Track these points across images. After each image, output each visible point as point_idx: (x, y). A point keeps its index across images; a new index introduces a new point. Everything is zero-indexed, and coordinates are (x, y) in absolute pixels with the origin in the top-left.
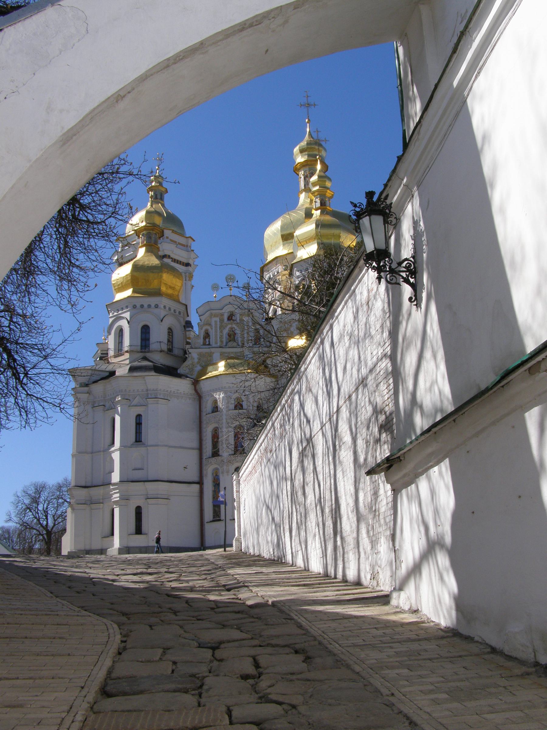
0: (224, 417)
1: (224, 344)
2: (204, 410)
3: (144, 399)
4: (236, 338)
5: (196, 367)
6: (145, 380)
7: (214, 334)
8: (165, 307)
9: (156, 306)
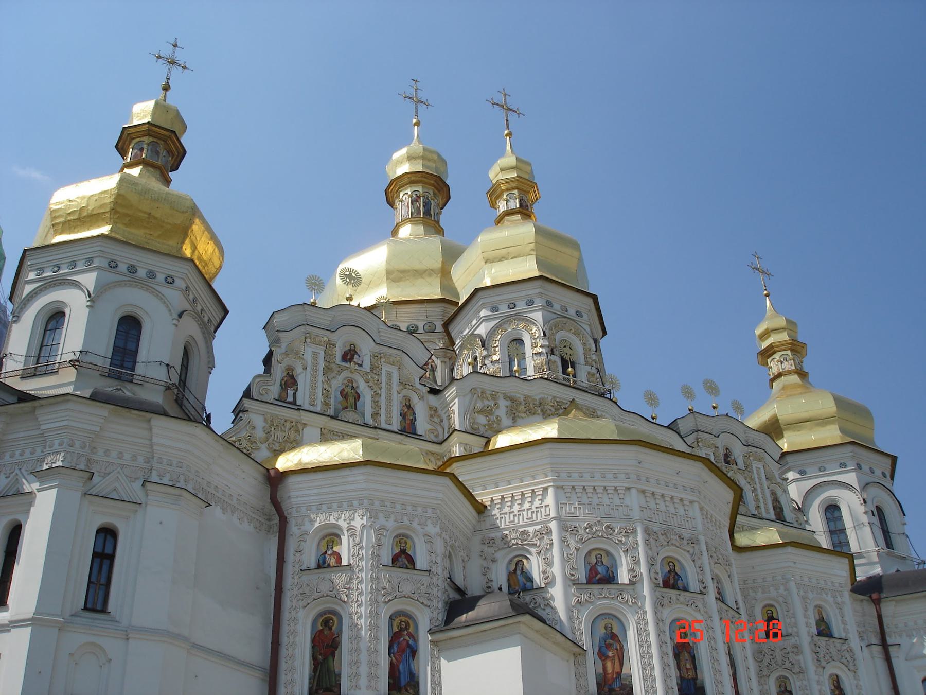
1: (331, 412)
2: (290, 556)
3: (137, 485)
4: (358, 404)
5: (258, 449)
6: (151, 429)
7: (308, 381)
8: (187, 289)
9: (170, 280)
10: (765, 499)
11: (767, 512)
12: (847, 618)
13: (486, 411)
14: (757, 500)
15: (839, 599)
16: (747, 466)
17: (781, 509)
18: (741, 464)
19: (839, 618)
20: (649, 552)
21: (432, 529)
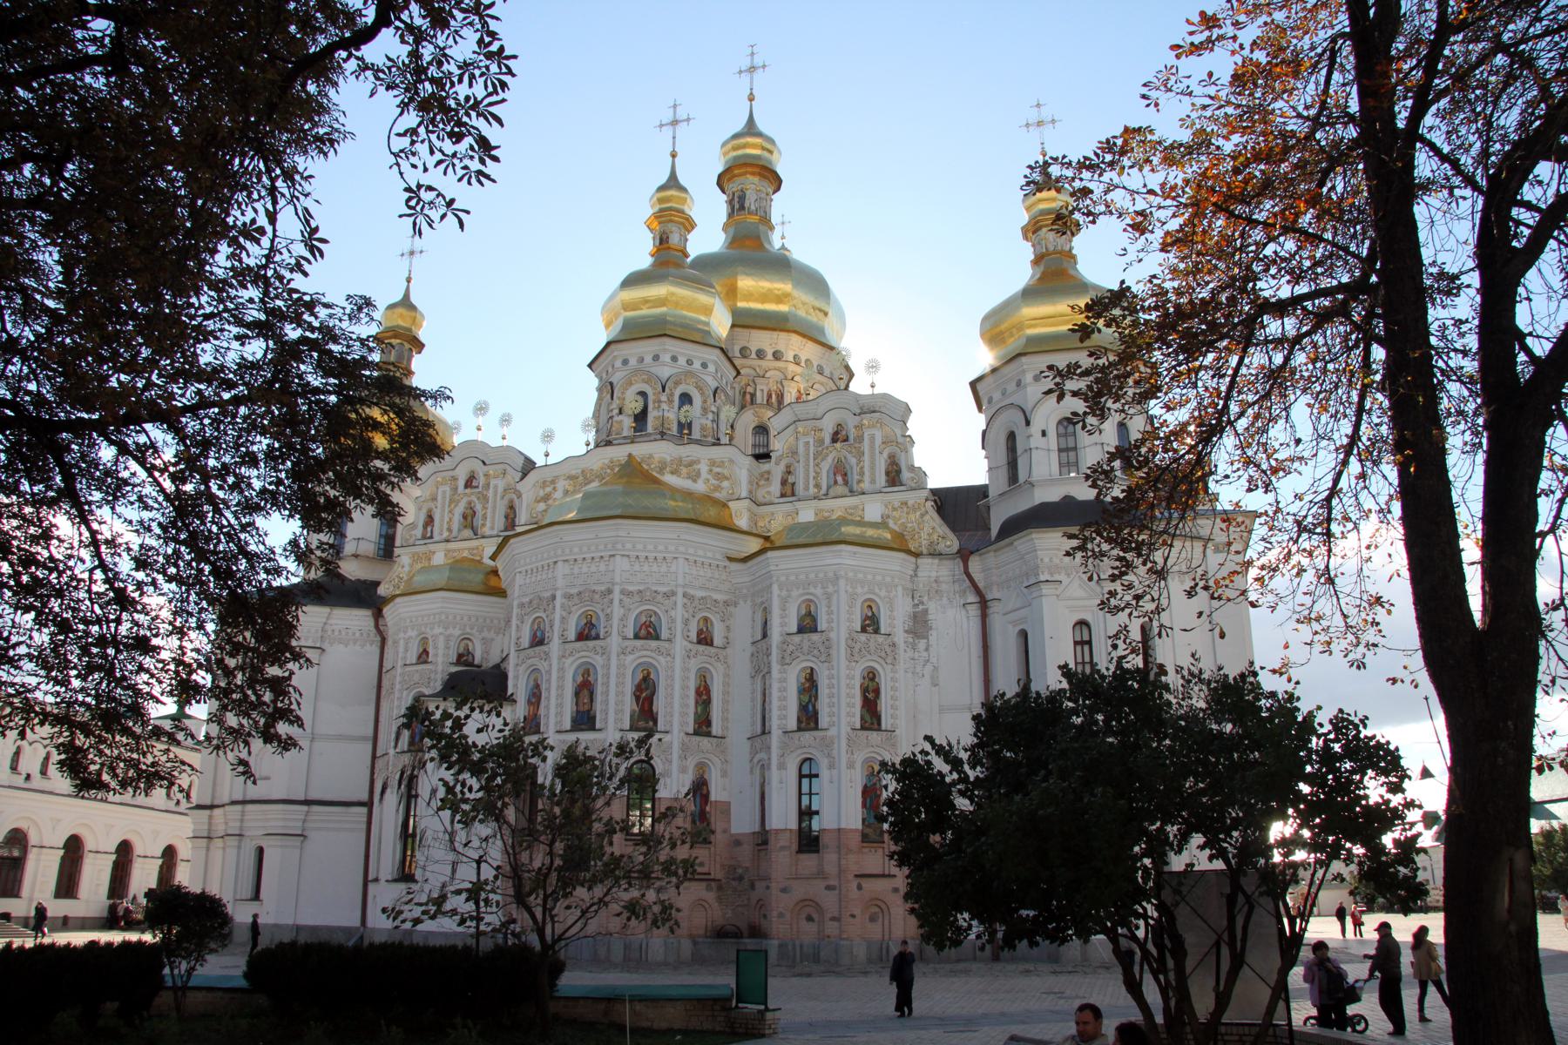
0: (398, 679)
10: (872, 468)
11: (873, 481)
12: (834, 608)
13: (546, 498)
14: (862, 474)
15: (830, 589)
16: (860, 439)
17: (899, 472)
18: (851, 438)
19: (824, 609)
20: (564, 614)
21: (438, 630)
